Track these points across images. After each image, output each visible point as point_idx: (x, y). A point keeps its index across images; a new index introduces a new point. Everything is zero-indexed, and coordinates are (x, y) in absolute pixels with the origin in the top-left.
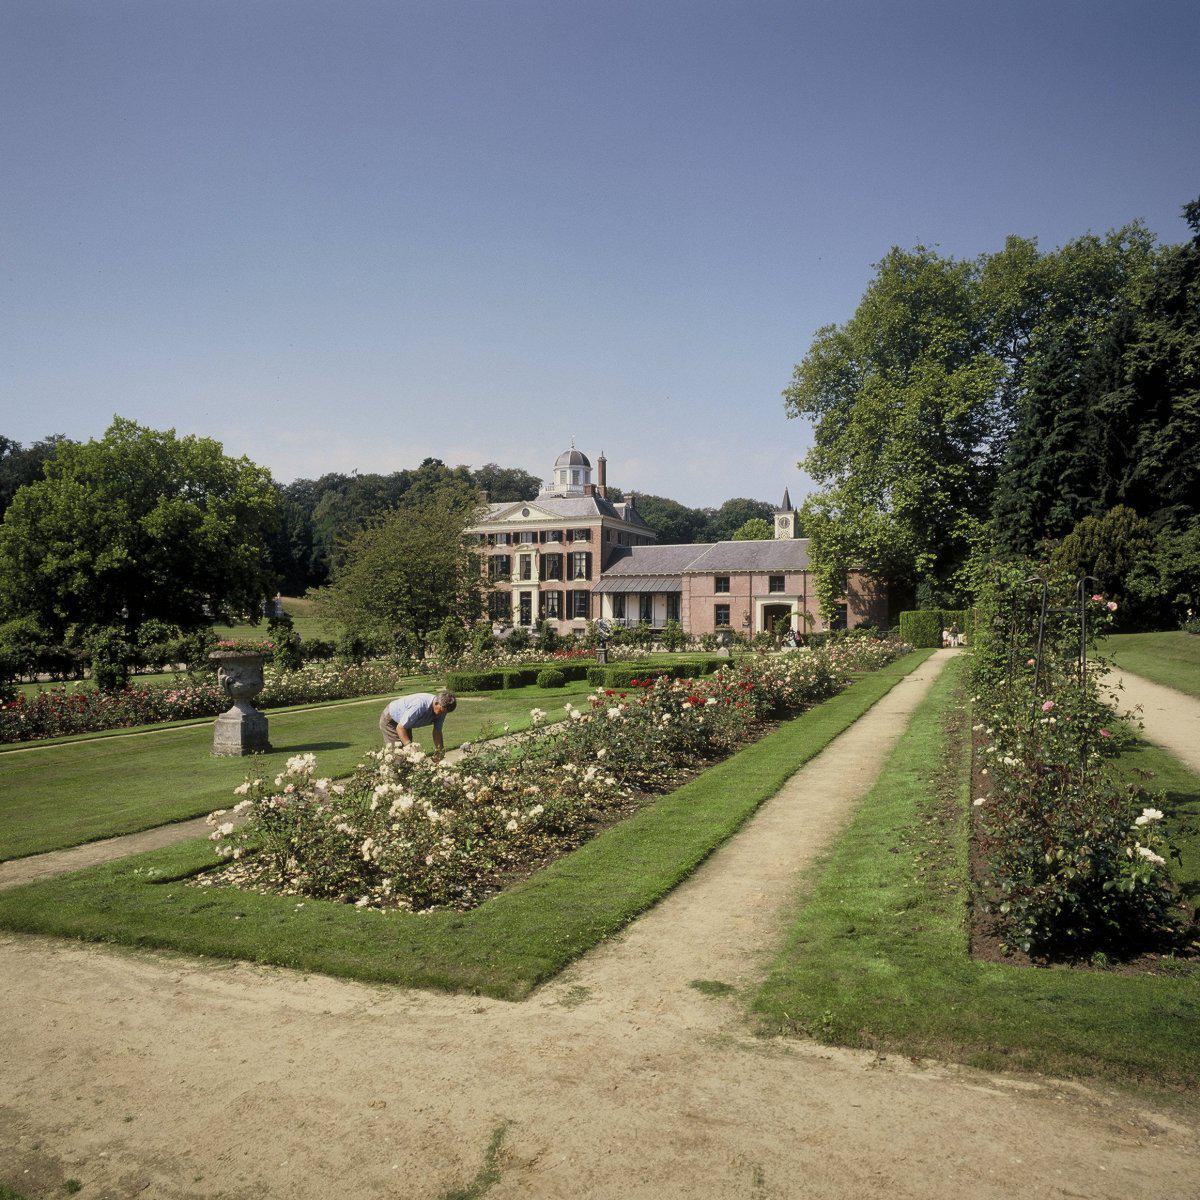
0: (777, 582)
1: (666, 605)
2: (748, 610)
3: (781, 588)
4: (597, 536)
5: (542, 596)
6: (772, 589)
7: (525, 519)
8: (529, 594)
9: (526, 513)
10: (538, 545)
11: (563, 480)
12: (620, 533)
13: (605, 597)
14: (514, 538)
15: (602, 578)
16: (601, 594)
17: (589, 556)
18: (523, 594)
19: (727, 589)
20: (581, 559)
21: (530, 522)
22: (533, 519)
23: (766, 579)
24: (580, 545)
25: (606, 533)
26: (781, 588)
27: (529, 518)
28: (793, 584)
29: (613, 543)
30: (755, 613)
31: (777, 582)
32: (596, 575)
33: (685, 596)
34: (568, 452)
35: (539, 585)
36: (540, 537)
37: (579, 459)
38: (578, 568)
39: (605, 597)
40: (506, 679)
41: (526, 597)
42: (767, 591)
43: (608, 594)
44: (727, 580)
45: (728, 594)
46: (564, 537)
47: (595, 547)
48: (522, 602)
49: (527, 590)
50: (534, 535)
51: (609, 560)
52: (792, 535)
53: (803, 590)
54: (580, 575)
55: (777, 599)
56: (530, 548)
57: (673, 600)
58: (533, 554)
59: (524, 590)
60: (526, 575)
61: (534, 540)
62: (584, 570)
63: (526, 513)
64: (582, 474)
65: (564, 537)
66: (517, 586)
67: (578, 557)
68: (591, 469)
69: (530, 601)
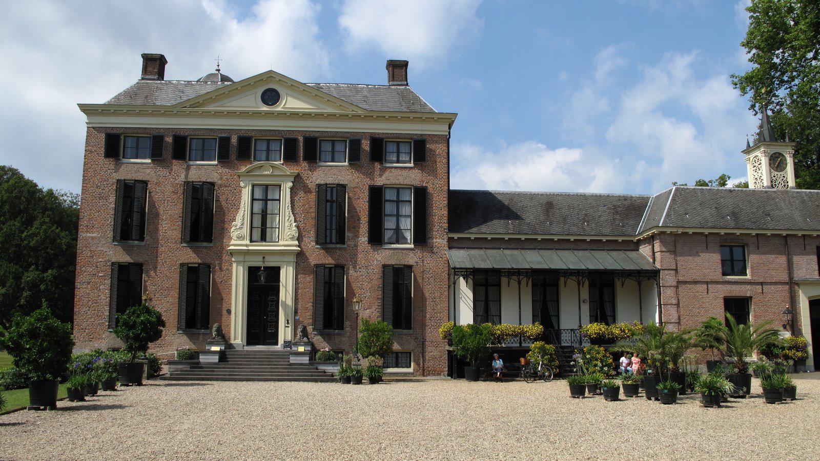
7: (265, 108)
8: (274, 273)
9: (271, 97)
10: (302, 167)
15: (450, 240)
17: (421, 195)
18: (253, 272)
20: (398, 202)
27: (279, 108)
32: (439, 240)
49: (271, 262)
52: (791, 182)
59: (257, 262)
61: (290, 156)
62: (407, 225)
66: (248, 253)
67: (389, 195)
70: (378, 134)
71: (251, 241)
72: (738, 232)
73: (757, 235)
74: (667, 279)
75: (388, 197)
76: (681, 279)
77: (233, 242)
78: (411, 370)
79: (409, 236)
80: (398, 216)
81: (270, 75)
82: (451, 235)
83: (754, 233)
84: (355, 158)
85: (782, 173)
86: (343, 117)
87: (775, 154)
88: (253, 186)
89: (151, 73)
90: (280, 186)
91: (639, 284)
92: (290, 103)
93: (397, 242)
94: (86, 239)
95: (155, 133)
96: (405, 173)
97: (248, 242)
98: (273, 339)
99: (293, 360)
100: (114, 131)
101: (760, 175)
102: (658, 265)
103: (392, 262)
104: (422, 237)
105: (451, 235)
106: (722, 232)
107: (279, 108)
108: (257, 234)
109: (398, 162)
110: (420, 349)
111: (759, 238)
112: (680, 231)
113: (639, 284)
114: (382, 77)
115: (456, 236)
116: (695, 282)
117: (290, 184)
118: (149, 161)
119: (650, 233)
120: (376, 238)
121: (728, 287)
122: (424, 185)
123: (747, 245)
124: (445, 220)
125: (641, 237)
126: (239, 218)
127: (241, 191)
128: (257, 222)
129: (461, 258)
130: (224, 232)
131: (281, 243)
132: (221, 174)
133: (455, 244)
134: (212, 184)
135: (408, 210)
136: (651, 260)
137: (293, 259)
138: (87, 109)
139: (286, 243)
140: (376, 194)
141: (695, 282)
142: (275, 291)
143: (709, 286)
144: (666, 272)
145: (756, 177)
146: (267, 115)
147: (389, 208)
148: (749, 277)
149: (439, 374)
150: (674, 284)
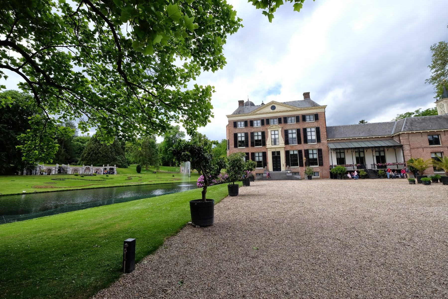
5: (287, 153)
7: (272, 111)
8: (279, 153)
9: (273, 108)
10: (283, 125)
14: (265, 122)
18: (273, 153)
20: (311, 131)
32: (324, 140)
35: (285, 148)
36: (283, 120)
41: (276, 157)
49: (278, 150)
58: (280, 130)
59: (274, 150)
60: (275, 142)
62: (314, 137)
63: (273, 108)
65: (301, 119)
66: (271, 148)
67: (308, 130)
70: (304, 114)
72: (435, 131)
73: (444, 131)
74: (406, 148)
77: (267, 146)
78: (319, 177)
80: (311, 135)
81: (273, 102)
83: (443, 130)
86: (293, 111)
88: (271, 131)
89: (241, 105)
90: (278, 130)
91: (395, 150)
92: (278, 108)
94: (231, 148)
95: (245, 120)
96: (312, 124)
97: (271, 145)
98: (280, 169)
99: (287, 174)
100: (235, 121)
101: (443, 110)
102: (402, 144)
105: (328, 140)
106: (428, 131)
107: (275, 110)
108: (273, 143)
109: (310, 121)
110: (321, 171)
111: (445, 132)
112: (410, 132)
113: (395, 150)
114: (302, 98)
115: (329, 140)
116: (418, 148)
117: (281, 130)
118: (244, 127)
119: (398, 134)
121: (432, 149)
123: (440, 134)
124: (326, 135)
125: (394, 135)
127: (268, 133)
129: (332, 146)
131: (280, 145)
132: (262, 129)
133: (329, 142)
135: (314, 134)
136: (399, 142)
137: (283, 149)
138: (228, 116)
139: (282, 145)
141: (418, 148)
142: (279, 157)
143: (424, 149)
144: (406, 146)
145: (442, 110)
147: (309, 134)
148: (441, 145)
149: (328, 178)
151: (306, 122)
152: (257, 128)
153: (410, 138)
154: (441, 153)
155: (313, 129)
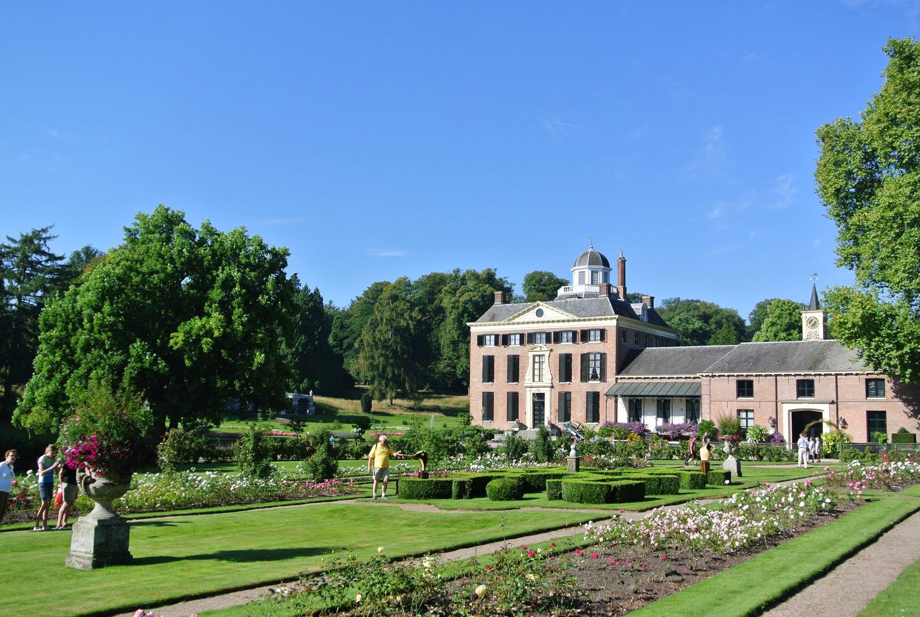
0: (805, 388)
1: (684, 409)
2: (774, 417)
3: (811, 393)
4: (612, 337)
6: (800, 393)
8: (541, 396)
9: (540, 313)
10: (552, 345)
11: (582, 281)
12: (637, 334)
13: (620, 400)
15: (617, 379)
16: (616, 396)
17: (603, 356)
19: (750, 393)
21: (543, 322)
22: (546, 320)
23: (793, 381)
24: (593, 346)
25: (622, 333)
26: (811, 393)
28: (824, 387)
29: (630, 344)
30: (782, 419)
31: (805, 388)
33: (705, 401)
34: (586, 254)
37: (597, 258)
38: (591, 370)
39: (620, 400)
40: (454, 489)
42: (796, 396)
43: (622, 396)
44: (750, 383)
45: (753, 399)
46: (579, 336)
47: (610, 348)
48: (534, 403)
49: (541, 391)
50: (548, 335)
51: (625, 362)
52: (821, 335)
53: (835, 396)
54: (595, 377)
55: (805, 405)
56: (541, 347)
57: (693, 405)
59: (536, 391)
61: (548, 340)
62: (598, 371)
63: (540, 313)
64: (600, 274)
65: (579, 336)
67: (592, 357)
68: (611, 270)
69: (543, 403)
71: (534, 381)
75: (591, 359)
76: (713, 399)
77: (526, 382)
79: (599, 376)
82: (617, 377)
84: (574, 340)
85: (815, 330)
87: (811, 317)
93: (595, 380)
97: (531, 382)
103: (591, 390)
104: (603, 378)
105: (617, 377)
108: (537, 378)
109: (595, 340)
115: (619, 377)
120: (584, 378)
122: (605, 352)
126: (528, 370)
128: (537, 372)
130: (524, 376)
134: (519, 356)
135: (598, 364)
140: (585, 358)
146: (538, 322)
147: (592, 364)
150: (709, 402)
151: (590, 342)
152: (513, 348)
153: (712, 384)
154: (752, 411)
155: (598, 357)
